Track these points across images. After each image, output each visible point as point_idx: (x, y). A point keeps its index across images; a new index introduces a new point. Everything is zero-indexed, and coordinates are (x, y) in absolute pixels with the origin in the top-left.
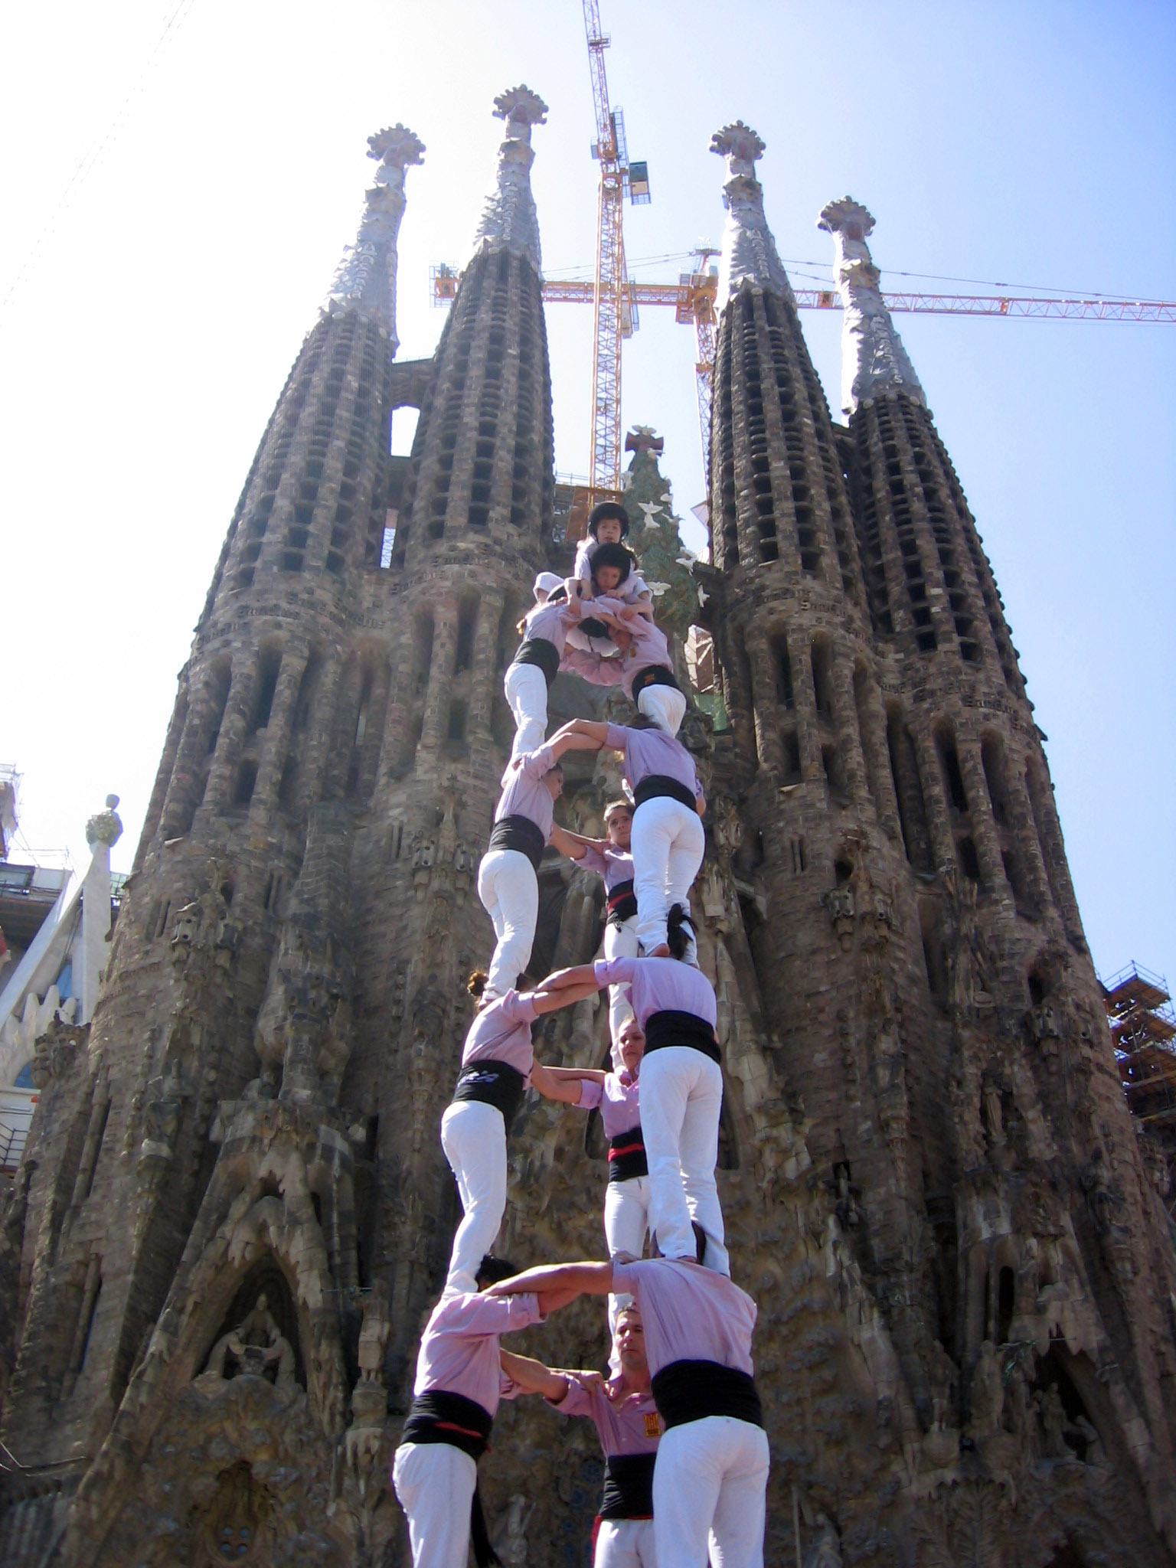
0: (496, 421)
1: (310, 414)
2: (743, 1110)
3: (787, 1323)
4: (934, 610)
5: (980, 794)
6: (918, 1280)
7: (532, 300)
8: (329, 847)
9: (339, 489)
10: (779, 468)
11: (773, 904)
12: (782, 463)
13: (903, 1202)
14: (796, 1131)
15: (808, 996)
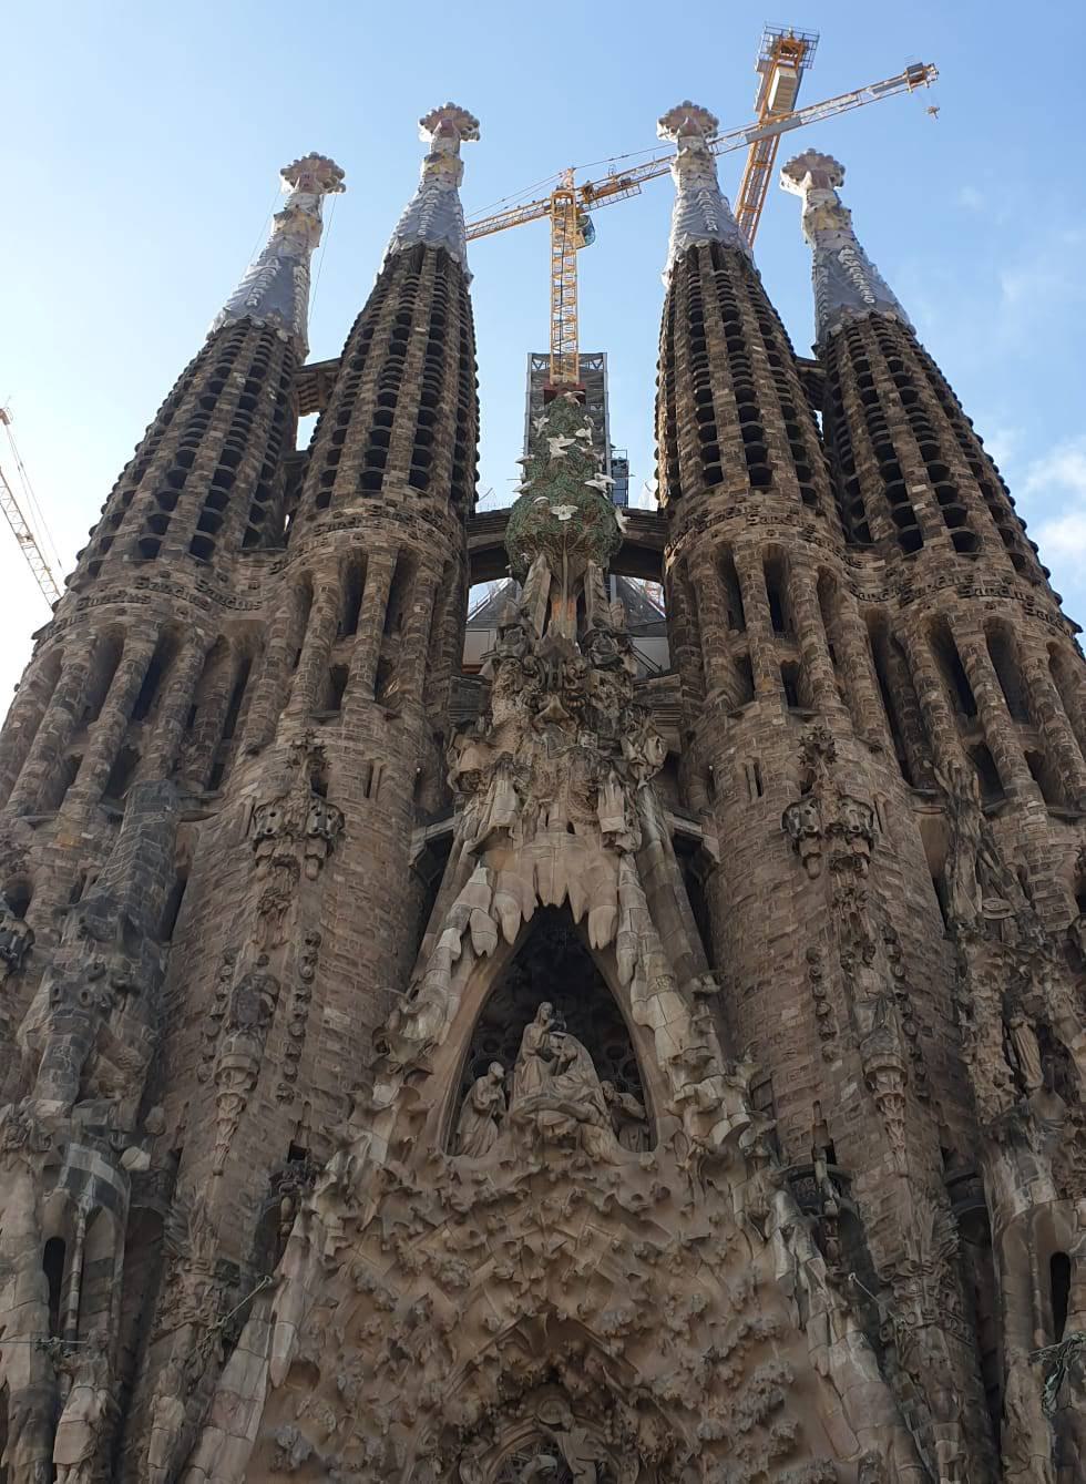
0: (398, 393)
1: (187, 410)
2: (656, 1063)
3: (727, 1358)
4: (916, 508)
5: (988, 689)
6: (933, 1288)
7: (450, 286)
8: (147, 826)
9: (212, 477)
10: (723, 396)
11: (726, 844)
12: (727, 391)
13: (905, 1180)
14: (728, 1086)
15: (771, 941)
